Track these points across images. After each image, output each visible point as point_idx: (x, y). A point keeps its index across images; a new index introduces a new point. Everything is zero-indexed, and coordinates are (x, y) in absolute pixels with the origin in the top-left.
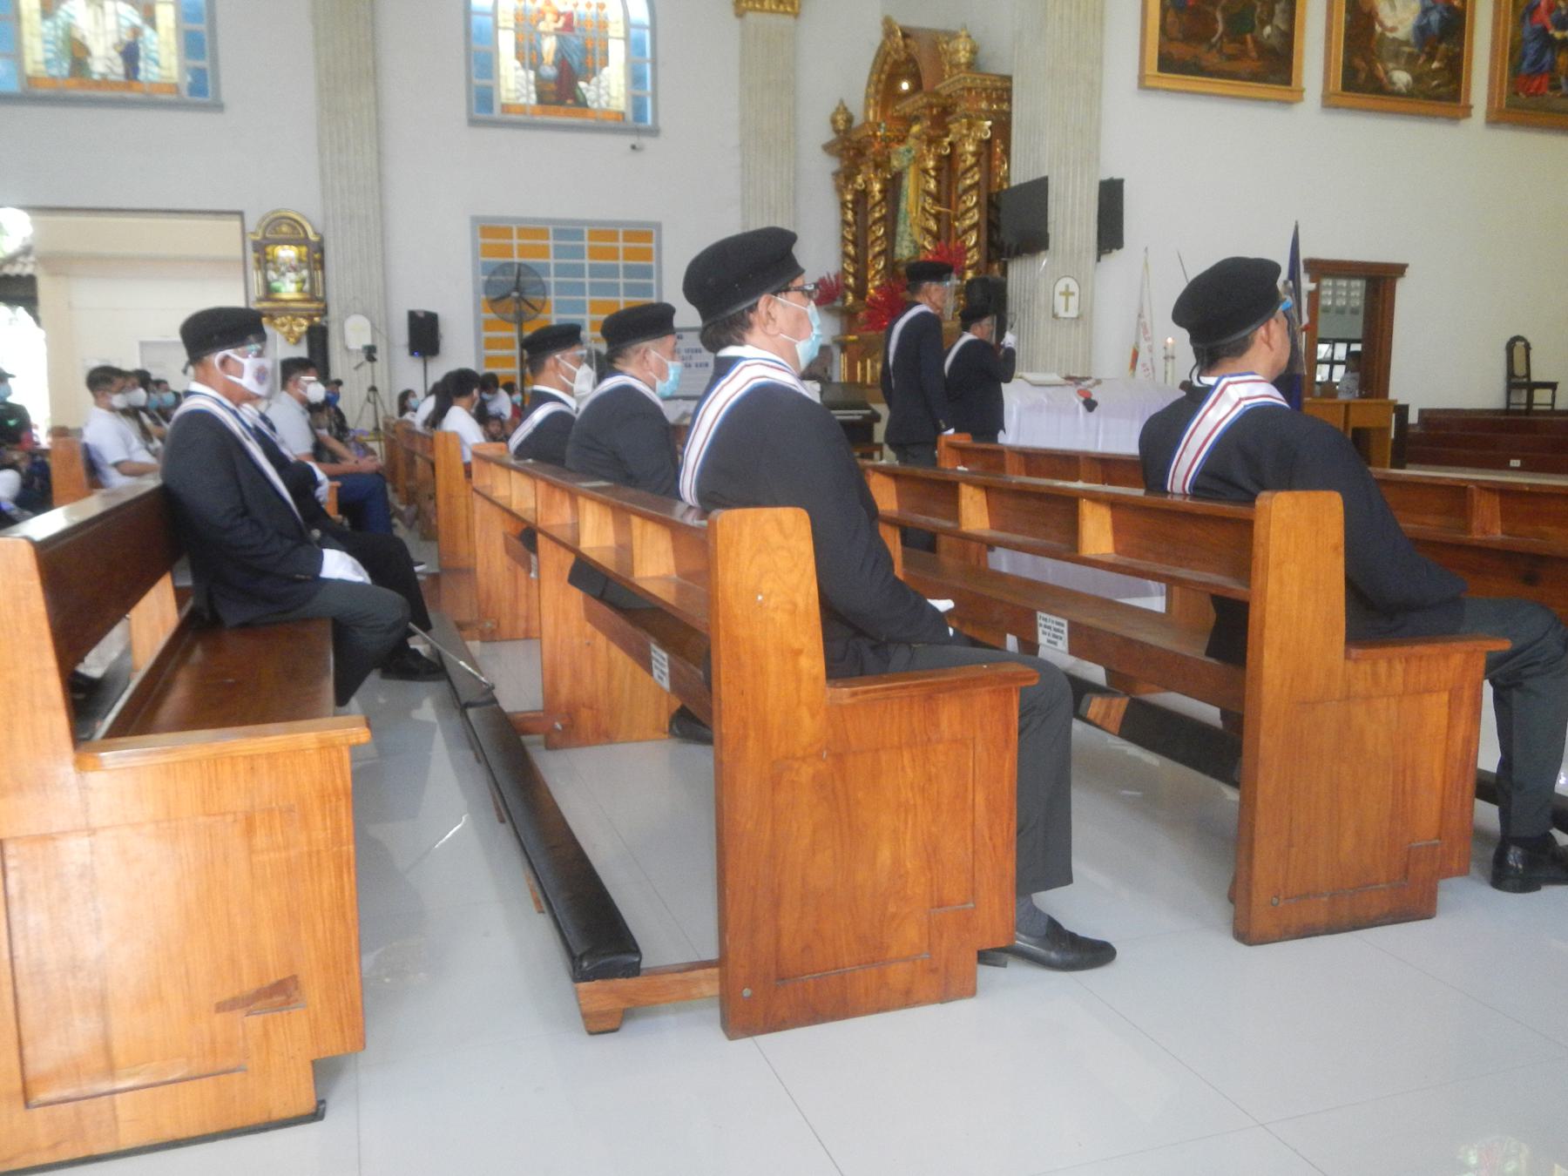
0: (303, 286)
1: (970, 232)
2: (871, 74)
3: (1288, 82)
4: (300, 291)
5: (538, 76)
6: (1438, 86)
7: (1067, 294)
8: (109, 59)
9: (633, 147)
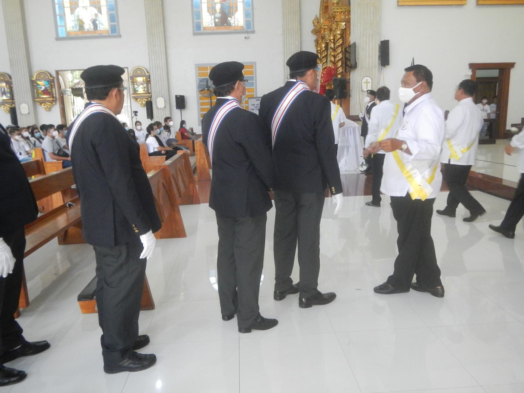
0: (145, 89)
2: (320, 7)
4: (144, 91)
7: (367, 83)
8: (90, 25)
9: (245, 38)
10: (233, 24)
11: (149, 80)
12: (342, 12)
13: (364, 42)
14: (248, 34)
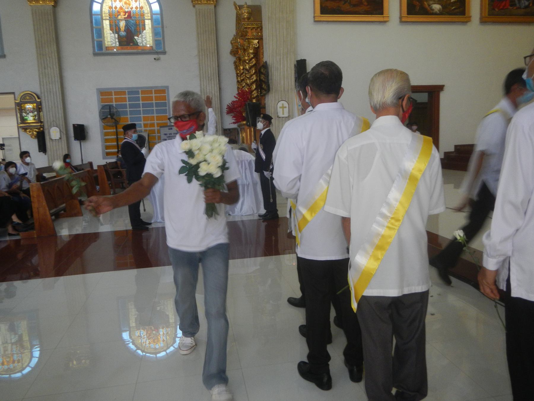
0: (36, 118)
1: (253, 85)
3: (382, 13)
4: (34, 119)
5: (118, 36)
6: (455, 9)
7: (283, 107)
9: (155, 59)
10: (140, 43)
11: (40, 107)
12: (253, 28)
13: (277, 61)
14: (158, 55)
